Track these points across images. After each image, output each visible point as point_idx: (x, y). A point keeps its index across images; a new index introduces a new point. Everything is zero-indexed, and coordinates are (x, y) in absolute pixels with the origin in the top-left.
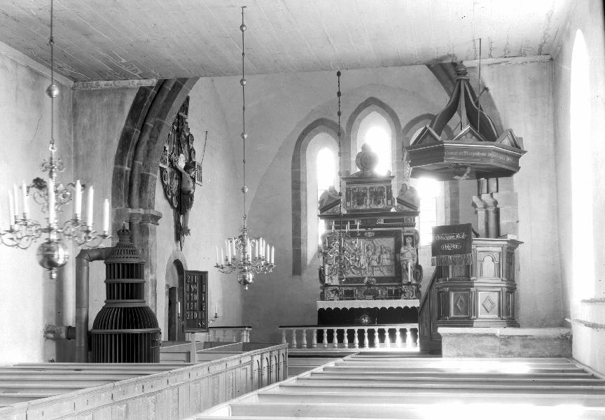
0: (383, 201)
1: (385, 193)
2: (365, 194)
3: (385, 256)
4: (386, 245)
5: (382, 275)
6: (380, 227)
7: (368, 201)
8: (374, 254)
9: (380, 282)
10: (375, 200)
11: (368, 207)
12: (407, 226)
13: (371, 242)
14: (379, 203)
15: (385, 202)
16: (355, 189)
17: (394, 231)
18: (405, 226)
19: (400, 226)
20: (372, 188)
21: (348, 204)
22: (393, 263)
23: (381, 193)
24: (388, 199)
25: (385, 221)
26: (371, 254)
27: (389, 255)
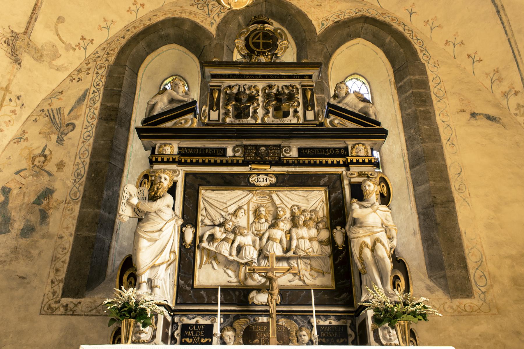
0: (296, 112)
1: (300, 96)
2: (252, 99)
3: (303, 232)
4: (303, 206)
5: (297, 283)
6: (288, 164)
7: (260, 112)
8: (273, 226)
9: (289, 304)
10: (277, 109)
11: (259, 121)
12: (358, 163)
13: (266, 201)
14: (286, 114)
15: (300, 114)
16: (230, 87)
17: (323, 175)
18: (352, 163)
19: (338, 165)
20: (270, 87)
21: (214, 115)
22: (328, 249)
23: (291, 97)
24: (305, 108)
25: (302, 152)
26: (266, 226)
27: (313, 232)
